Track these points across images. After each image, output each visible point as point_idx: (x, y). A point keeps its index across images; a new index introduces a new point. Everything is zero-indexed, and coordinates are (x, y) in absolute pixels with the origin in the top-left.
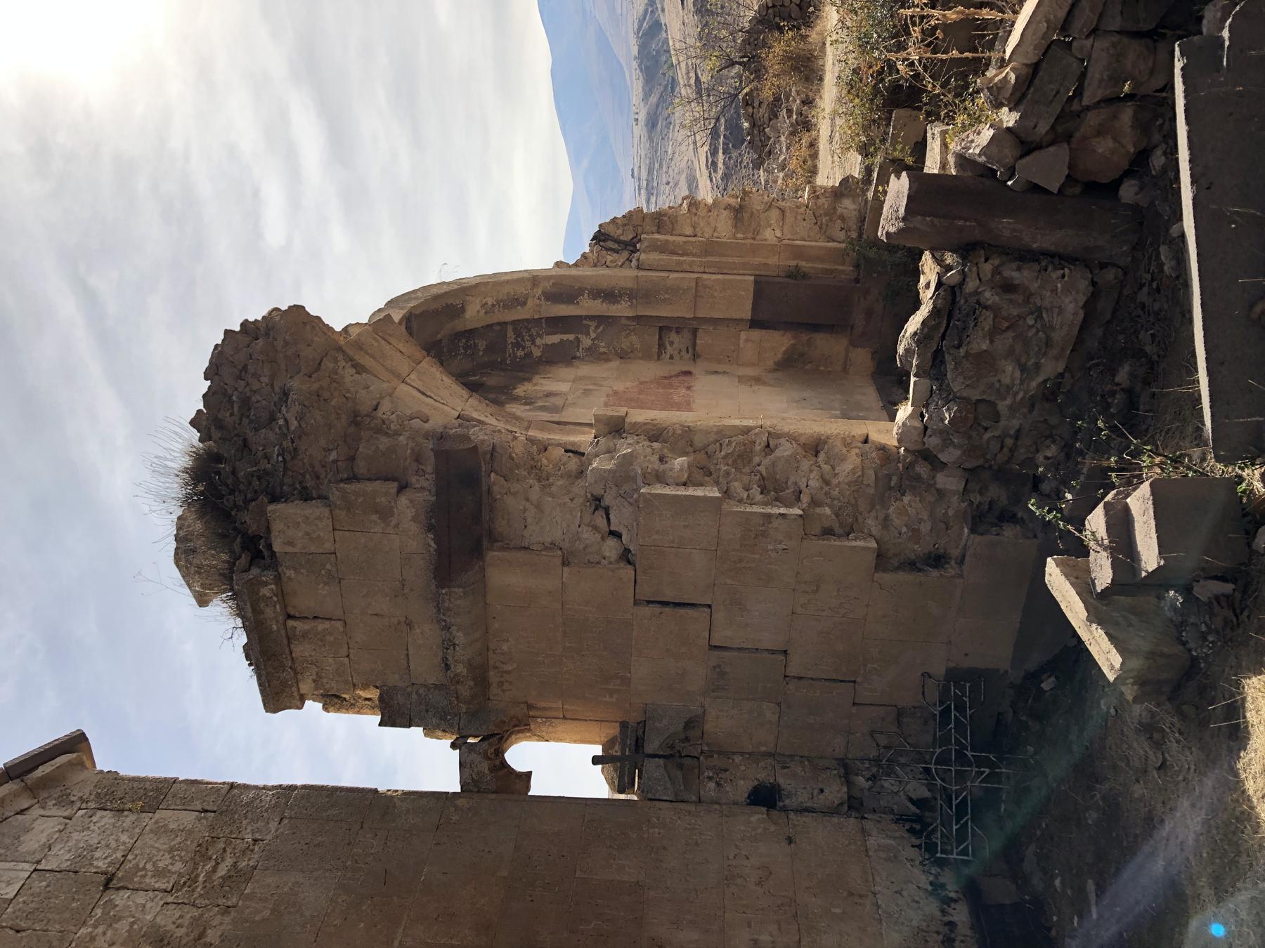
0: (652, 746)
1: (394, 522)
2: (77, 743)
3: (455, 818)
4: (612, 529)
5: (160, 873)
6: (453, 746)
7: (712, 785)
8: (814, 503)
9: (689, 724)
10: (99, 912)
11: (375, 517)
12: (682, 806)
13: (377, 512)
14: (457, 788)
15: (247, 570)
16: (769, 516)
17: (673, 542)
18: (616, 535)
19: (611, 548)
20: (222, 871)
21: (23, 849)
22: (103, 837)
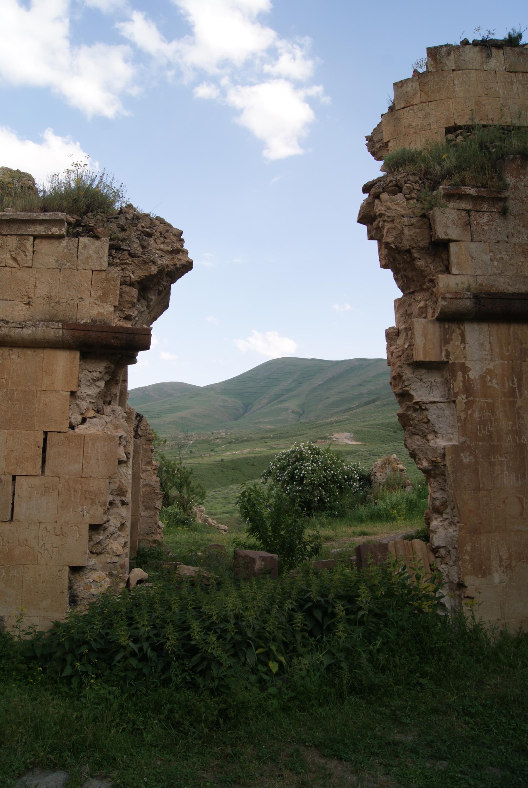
1: (98, 303)
4: (88, 420)
11: (100, 293)
13: (104, 294)
17: (87, 453)
18: (84, 421)
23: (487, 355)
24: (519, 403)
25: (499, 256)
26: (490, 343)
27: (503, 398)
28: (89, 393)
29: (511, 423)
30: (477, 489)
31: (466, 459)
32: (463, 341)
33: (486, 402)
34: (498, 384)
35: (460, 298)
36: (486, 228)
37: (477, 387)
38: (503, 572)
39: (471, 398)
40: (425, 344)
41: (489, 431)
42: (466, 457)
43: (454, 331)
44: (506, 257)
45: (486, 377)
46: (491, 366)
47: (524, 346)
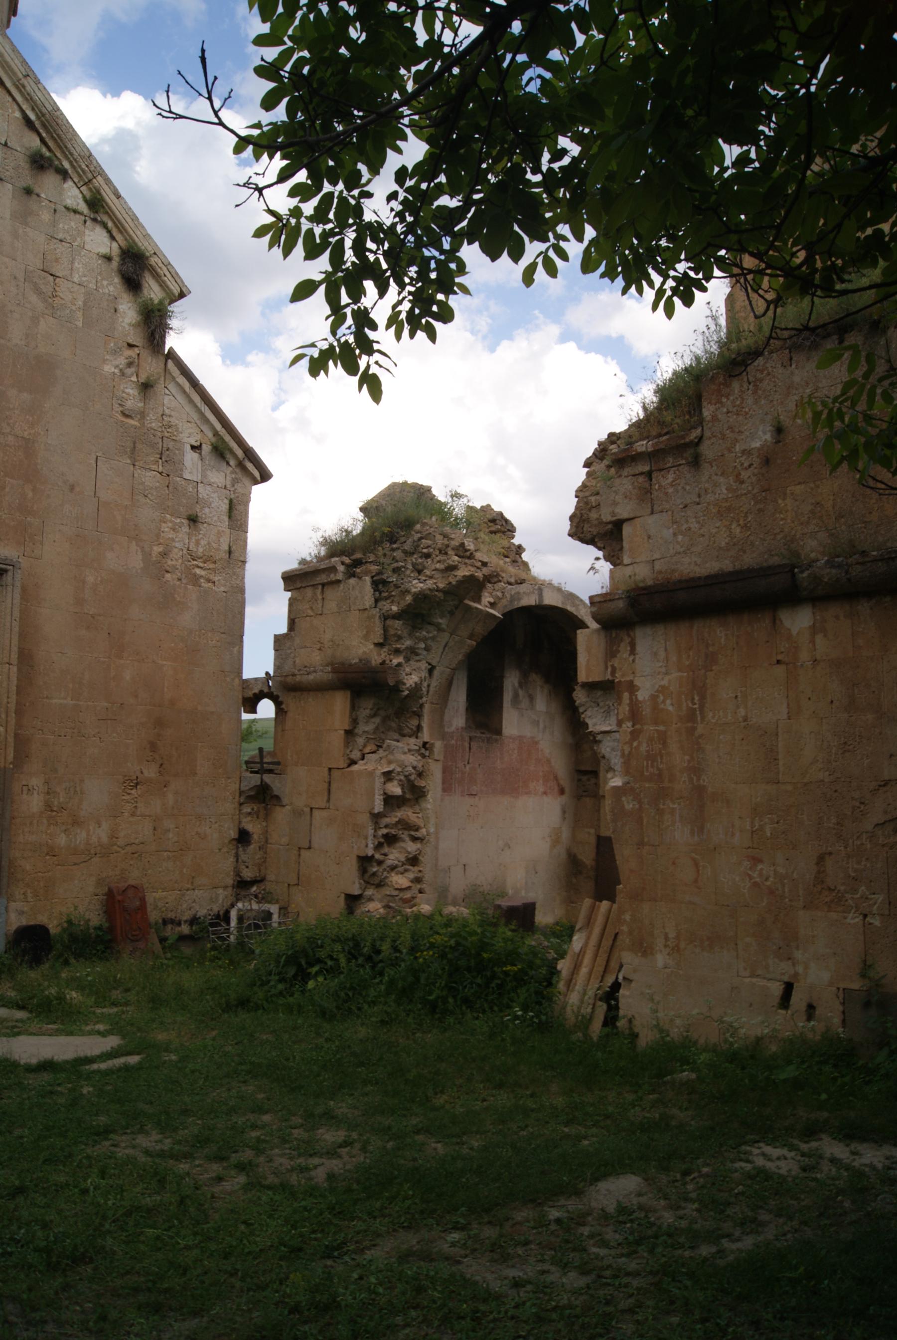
0: (267, 778)
2: (265, 476)
3: (228, 679)
5: (198, 543)
6: (267, 673)
7: (249, 810)
8: (380, 863)
9: (277, 798)
10: (178, 521)
11: (365, 632)
12: (238, 795)
14: (245, 677)
15: (343, 563)
16: (366, 838)
19: (356, 755)
20: (198, 571)
21: (209, 473)
22: (215, 509)
23: (661, 667)
24: (700, 729)
25: (685, 526)
26: (666, 650)
27: (679, 724)
28: (366, 729)
29: (687, 757)
30: (641, 844)
31: (629, 805)
32: (633, 652)
33: (657, 730)
34: (672, 704)
35: (610, 600)
36: (671, 490)
37: (647, 711)
38: (668, 954)
39: (638, 727)
40: (588, 660)
41: (658, 769)
42: (628, 802)
43: (622, 640)
44: (694, 526)
45: (658, 696)
46: (665, 682)
47: (711, 649)
